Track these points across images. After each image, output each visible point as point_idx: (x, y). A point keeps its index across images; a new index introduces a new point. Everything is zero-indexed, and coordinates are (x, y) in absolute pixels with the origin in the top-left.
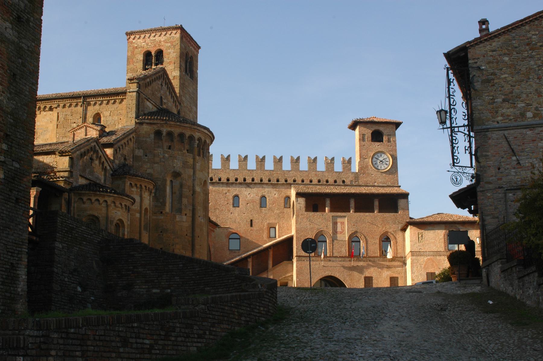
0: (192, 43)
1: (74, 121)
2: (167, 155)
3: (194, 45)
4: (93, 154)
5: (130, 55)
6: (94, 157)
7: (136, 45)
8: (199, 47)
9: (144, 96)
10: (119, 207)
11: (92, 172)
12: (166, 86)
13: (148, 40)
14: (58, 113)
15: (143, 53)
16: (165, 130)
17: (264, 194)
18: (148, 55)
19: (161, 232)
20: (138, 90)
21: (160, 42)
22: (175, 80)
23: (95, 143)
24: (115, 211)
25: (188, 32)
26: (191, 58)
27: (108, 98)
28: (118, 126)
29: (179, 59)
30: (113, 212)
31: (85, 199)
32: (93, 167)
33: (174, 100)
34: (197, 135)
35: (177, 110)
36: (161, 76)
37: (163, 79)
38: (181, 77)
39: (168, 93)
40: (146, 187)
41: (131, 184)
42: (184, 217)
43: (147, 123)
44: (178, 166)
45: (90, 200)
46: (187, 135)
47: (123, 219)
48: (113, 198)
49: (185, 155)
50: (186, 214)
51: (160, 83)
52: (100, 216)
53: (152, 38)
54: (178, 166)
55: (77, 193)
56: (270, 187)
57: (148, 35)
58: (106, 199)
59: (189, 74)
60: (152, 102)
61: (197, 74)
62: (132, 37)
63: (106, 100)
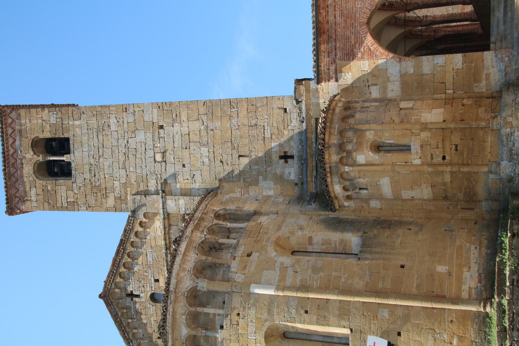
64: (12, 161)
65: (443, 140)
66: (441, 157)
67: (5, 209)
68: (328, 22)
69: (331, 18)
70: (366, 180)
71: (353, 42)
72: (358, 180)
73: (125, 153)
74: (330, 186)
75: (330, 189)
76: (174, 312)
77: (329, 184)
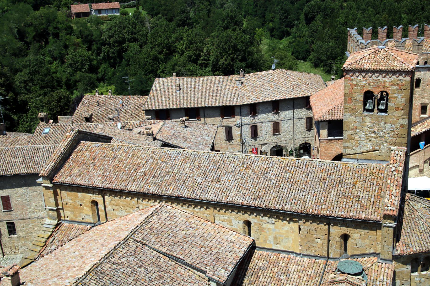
1: (318, 236)
2: (423, 279)
5: (347, 92)
7: (355, 83)
13: (370, 80)
14: (300, 226)
15: (363, 92)
17: (419, 77)
18: (368, 95)
28: (369, 250)
53: (374, 77)
56: (425, 70)
57: (370, 75)
62: (351, 74)
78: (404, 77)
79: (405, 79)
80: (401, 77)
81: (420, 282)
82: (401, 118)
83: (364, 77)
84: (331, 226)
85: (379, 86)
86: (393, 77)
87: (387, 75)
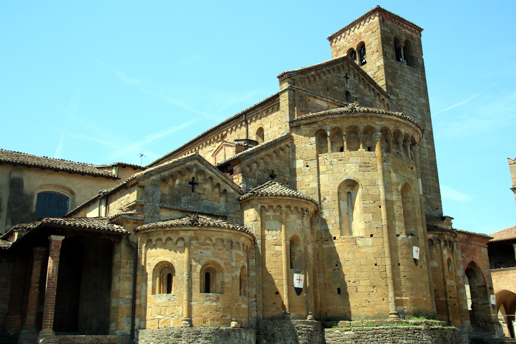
0: (405, 26)
2: (335, 160)
3: (409, 28)
4: (197, 176)
6: (200, 179)
7: (339, 47)
8: (420, 30)
9: (305, 93)
10: (209, 245)
11: (198, 200)
12: (357, 78)
13: (348, 37)
16: (328, 128)
19: (337, 265)
20: (290, 86)
21: (360, 33)
22: (380, 71)
23: (196, 162)
24: (200, 251)
25: (393, 12)
26: (407, 42)
27: (266, 108)
29: (381, 45)
30: (196, 252)
31: (154, 239)
32: (200, 194)
33: (374, 94)
34: (378, 125)
35: (384, 105)
36: (343, 67)
37: (349, 70)
38: (387, 66)
39: (362, 87)
40: (289, 207)
41: (263, 207)
42: (370, 241)
43: (305, 125)
44: (352, 170)
45: (160, 239)
46: (362, 129)
47: (218, 261)
48: (193, 232)
49: (362, 154)
50: (372, 236)
51: (343, 74)
52: (175, 261)
53: (352, 33)
54: (352, 170)
55: (144, 233)
58: (182, 234)
59: (405, 61)
60: (324, 99)
61: (423, 60)
62: (334, 40)
63: (265, 110)
64: (401, 23)
65: (456, 297)
66: (451, 296)
67: (381, 7)
68: (472, 241)
69: (473, 242)
70: (435, 253)
71: (467, 253)
72: (435, 249)
73: (411, 102)
74: (433, 232)
75: (432, 232)
76: (410, 127)
77: (436, 232)
78: (373, 19)
79: (374, 20)
80: (371, 21)
81: (331, 163)
82: (377, 60)
83: (344, 38)
84: (249, 127)
85: (356, 40)
86: (365, 24)
87: (360, 24)
